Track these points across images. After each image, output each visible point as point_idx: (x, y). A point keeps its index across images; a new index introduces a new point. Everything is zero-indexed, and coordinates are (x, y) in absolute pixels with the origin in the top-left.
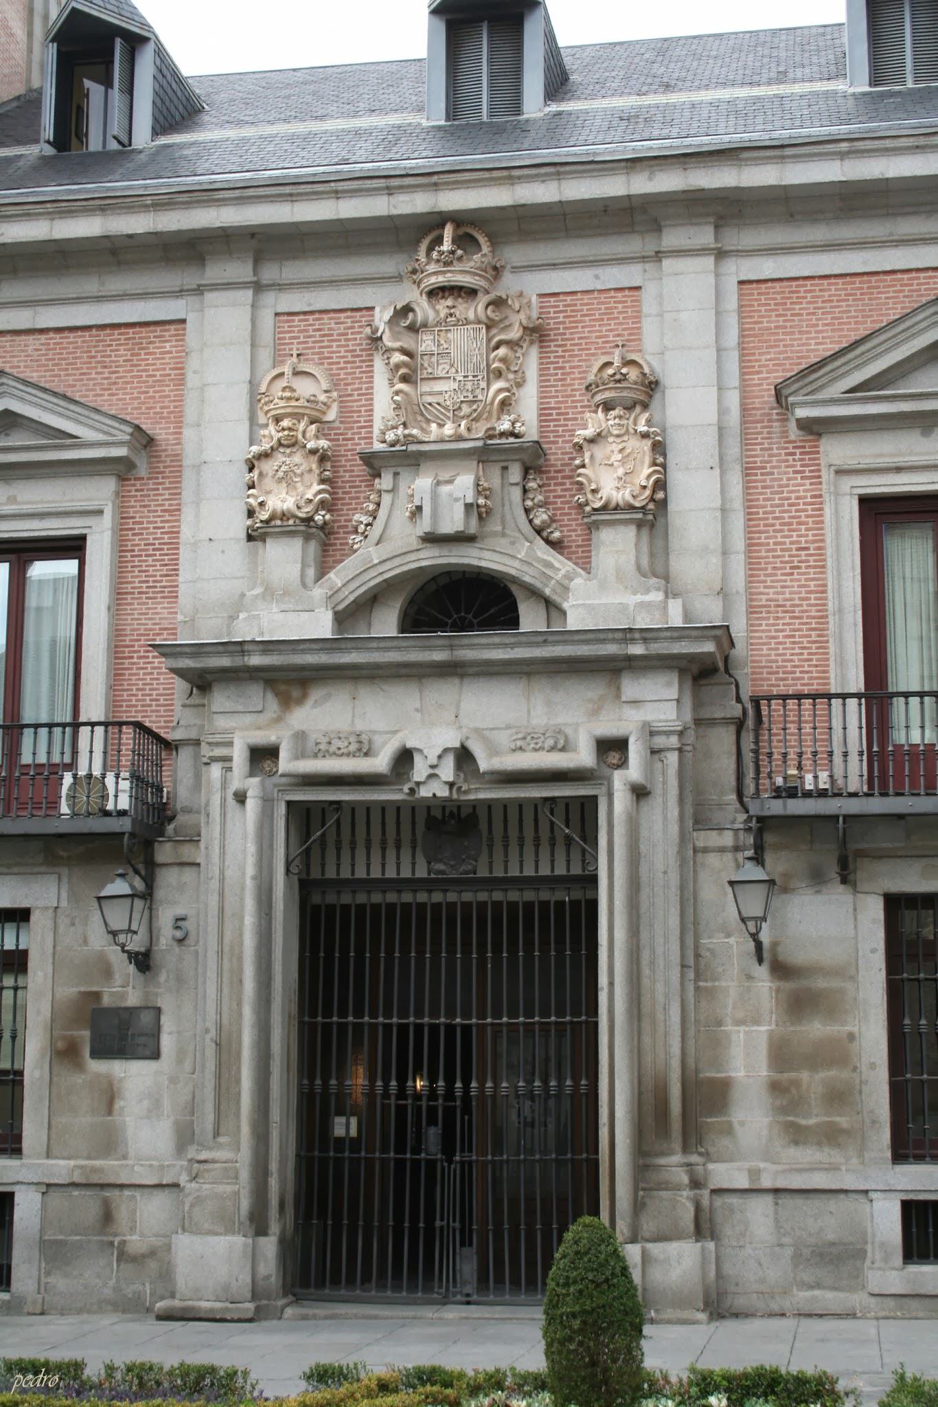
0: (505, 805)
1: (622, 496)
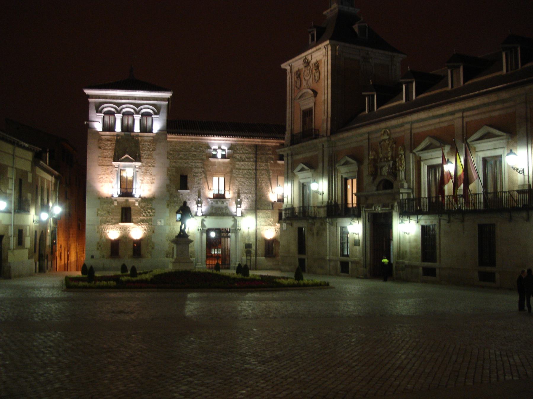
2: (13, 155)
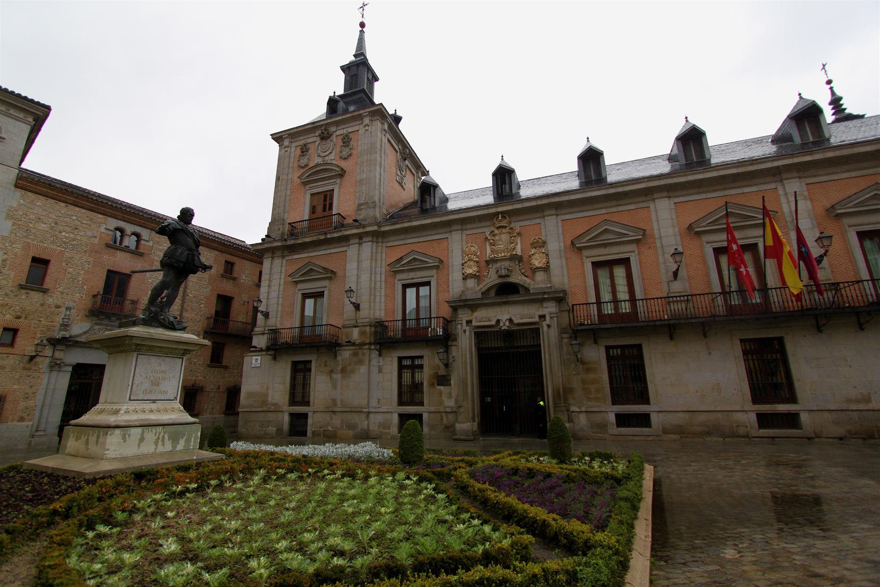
0: (519, 330)
1: (541, 265)
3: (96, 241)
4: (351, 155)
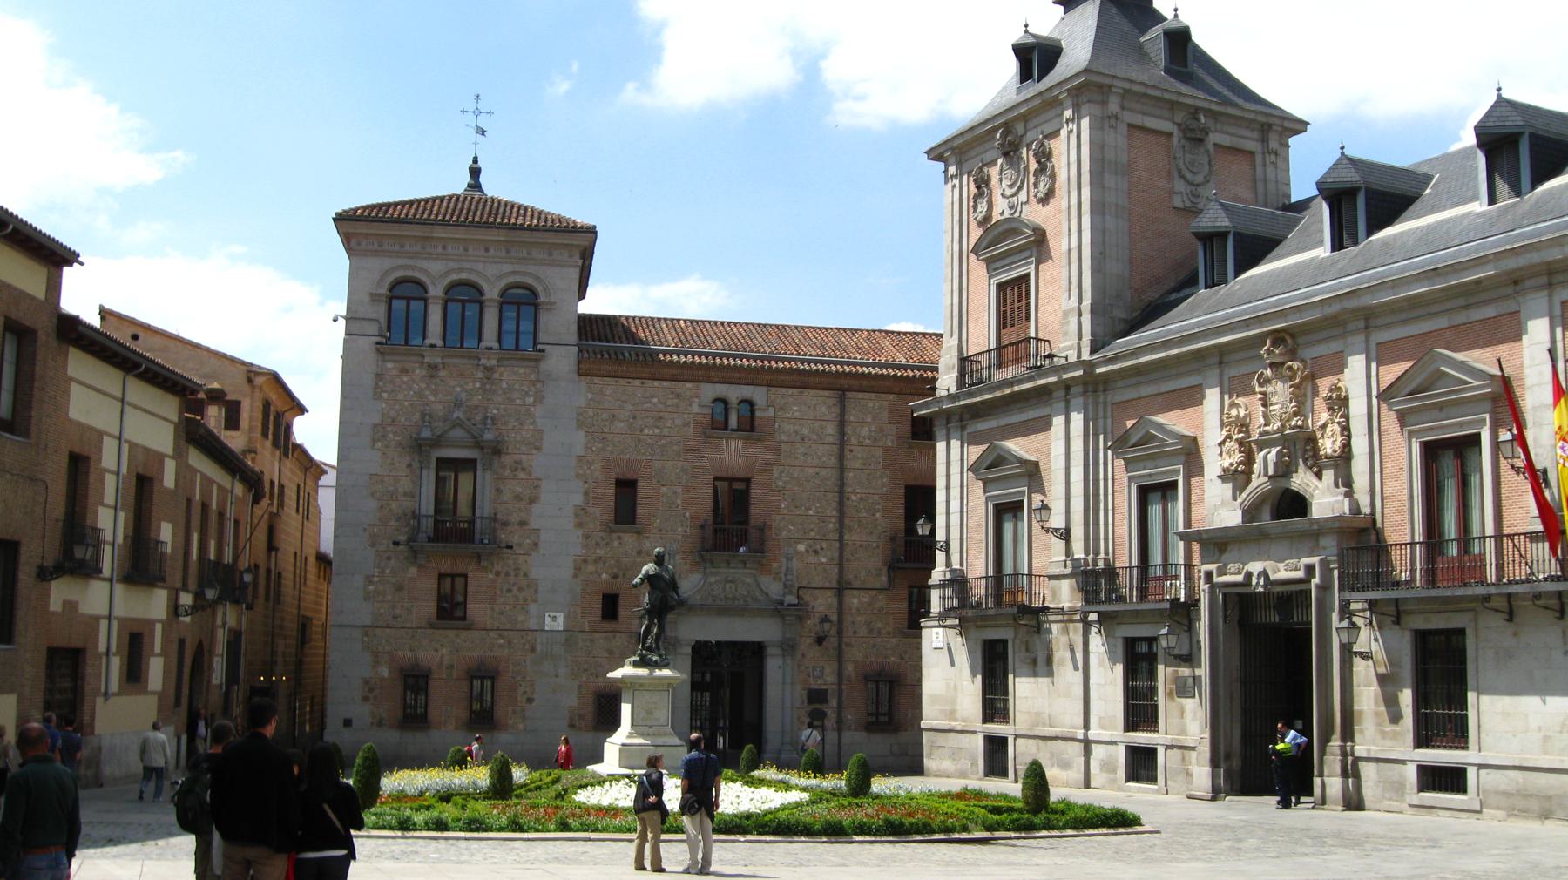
2: (122, 401)
3: (690, 431)
4: (1050, 194)
